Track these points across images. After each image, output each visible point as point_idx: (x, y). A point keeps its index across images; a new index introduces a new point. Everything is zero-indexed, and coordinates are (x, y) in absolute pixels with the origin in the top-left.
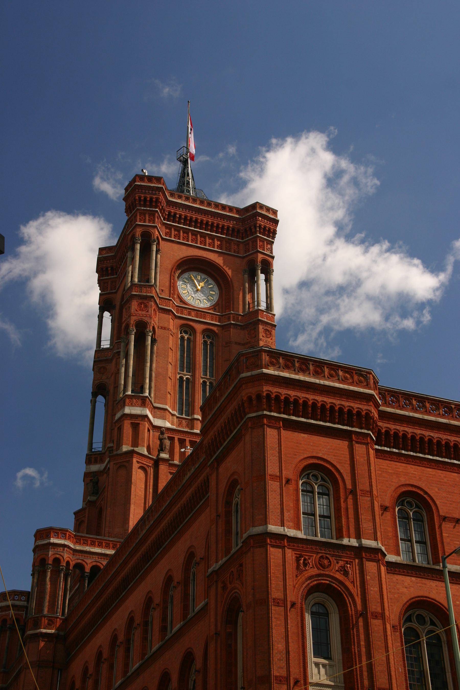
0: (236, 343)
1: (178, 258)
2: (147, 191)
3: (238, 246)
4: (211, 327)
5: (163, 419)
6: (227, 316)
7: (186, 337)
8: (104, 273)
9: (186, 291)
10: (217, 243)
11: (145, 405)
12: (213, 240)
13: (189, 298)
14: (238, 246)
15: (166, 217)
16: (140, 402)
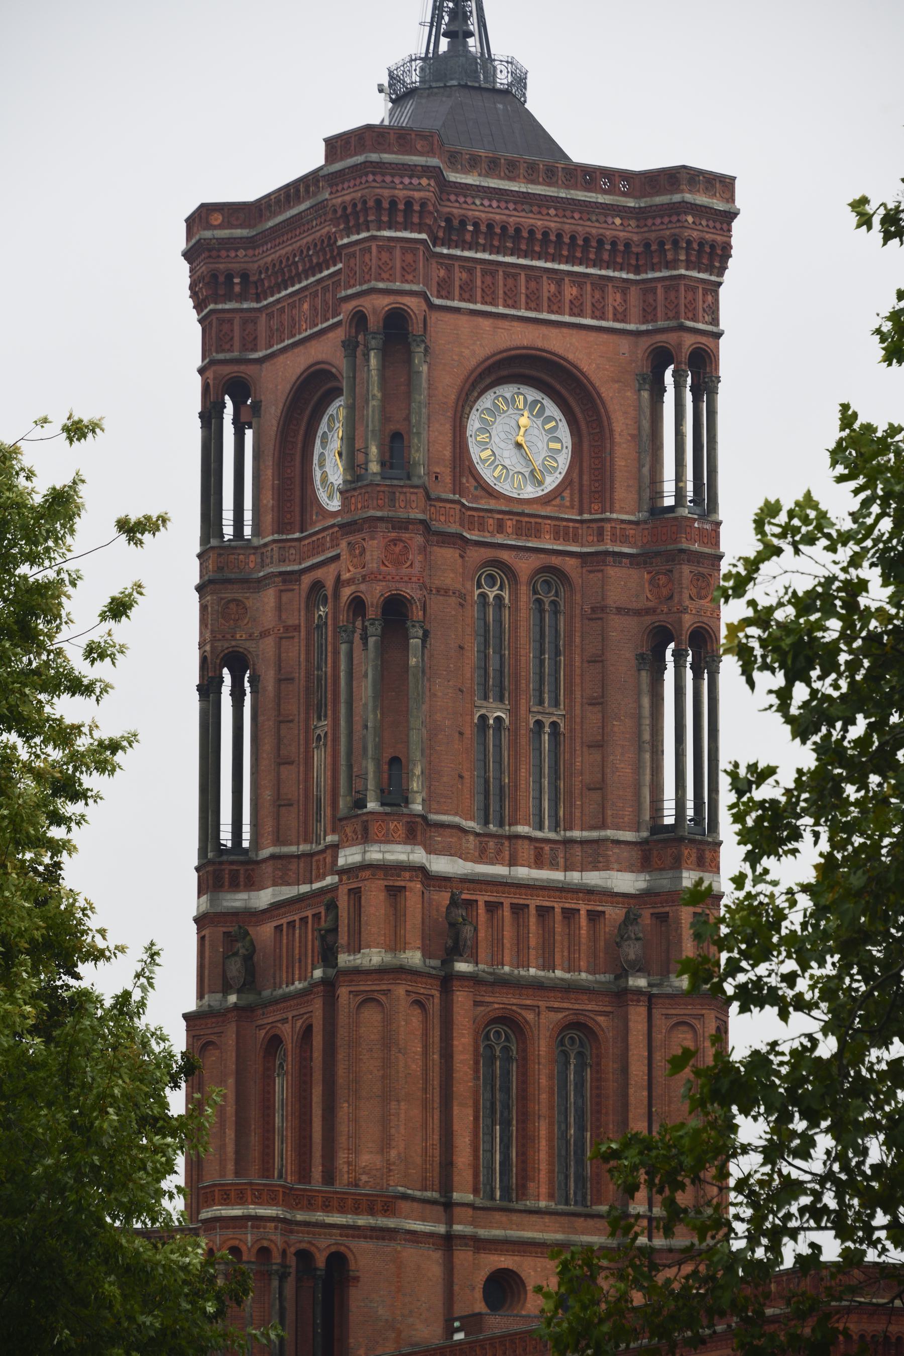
0: (619, 610)
1: (473, 362)
2: (397, 180)
3: (624, 292)
4: (555, 561)
5: (451, 855)
6: (594, 525)
7: (491, 596)
8: (221, 292)
9: (489, 452)
10: (569, 292)
11: (415, 837)
12: (559, 283)
13: (496, 474)
14: (624, 292)
15: (441, 234)
16: (402, 831)
